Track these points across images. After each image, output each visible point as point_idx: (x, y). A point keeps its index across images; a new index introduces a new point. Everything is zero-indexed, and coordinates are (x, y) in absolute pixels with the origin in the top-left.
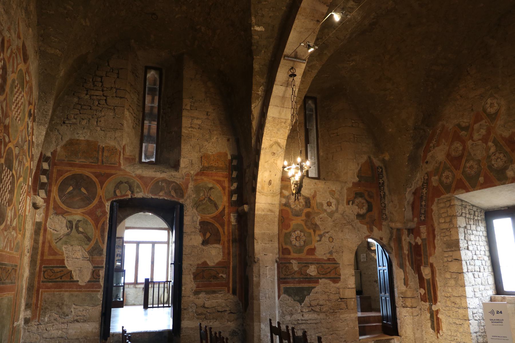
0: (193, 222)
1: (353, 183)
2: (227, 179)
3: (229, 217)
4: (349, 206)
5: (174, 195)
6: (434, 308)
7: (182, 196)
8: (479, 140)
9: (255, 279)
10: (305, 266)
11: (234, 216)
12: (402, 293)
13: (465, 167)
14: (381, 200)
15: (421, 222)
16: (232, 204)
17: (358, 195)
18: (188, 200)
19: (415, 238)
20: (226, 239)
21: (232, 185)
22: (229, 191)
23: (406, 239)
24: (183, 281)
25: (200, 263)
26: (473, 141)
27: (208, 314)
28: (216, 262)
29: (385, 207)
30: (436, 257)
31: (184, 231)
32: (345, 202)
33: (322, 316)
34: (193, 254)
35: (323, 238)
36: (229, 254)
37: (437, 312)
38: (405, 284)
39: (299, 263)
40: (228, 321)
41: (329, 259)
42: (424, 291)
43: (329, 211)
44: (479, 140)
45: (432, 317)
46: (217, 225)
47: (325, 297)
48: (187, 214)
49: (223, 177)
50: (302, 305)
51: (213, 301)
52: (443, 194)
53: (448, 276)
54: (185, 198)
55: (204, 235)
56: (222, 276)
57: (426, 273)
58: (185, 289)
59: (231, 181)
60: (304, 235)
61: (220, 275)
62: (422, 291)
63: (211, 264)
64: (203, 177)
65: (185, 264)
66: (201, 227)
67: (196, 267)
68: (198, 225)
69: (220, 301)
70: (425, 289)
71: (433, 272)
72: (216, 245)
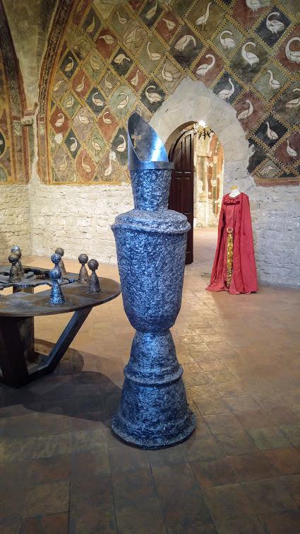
15: (214, 154)
23: (207, 164)
45: (214, 206)
62: (210, 193)
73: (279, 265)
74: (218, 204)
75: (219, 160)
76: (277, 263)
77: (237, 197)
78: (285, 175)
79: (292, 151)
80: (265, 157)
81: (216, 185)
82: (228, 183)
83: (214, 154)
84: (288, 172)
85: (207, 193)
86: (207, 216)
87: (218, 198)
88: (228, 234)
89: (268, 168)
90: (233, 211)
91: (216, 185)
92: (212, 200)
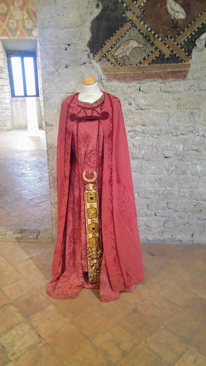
8: (18, 7)
13: (8, 22)
26: (14, 6)
44: (18, 7)
73: (148, 212)
76: (146, 210)
77: (101, 103)
78: (161, 59)
79: (177, 7)
80: (124, 20)
82: (52, 73)
84: (167, 53)
88: (86, 183)
89: (129, 45)
90: (95, 137)
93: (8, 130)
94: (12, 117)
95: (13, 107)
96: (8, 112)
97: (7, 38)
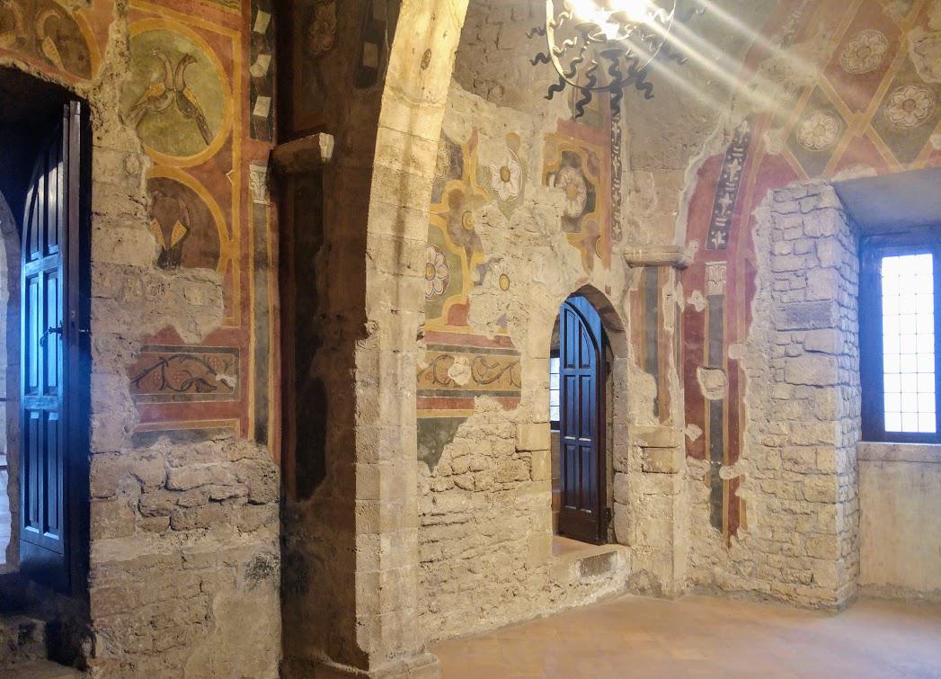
0: (127, 175)
1: (560, 122)
2: (239, 35)
3: (245, 177)
4: (547, 189)
5: (56, 59)
6: (726, 473)
7: (87, 71)
9: (360, 391)
10: (445, 357)
11: (259, 173)
12: (644, 436)
14: (613, 182)
15: (709, 252)
16: (254, 129)
17: (570, 159)
18: (107, 88)
19: (687, 293)
20: (236, 254)
21: (254, 60)
22: (243, 78)
23: (672, 296)
24: (96, 396)
25: (153, 332)
27: (181, 511)
28: (206, 329)
29: (619, 203)
30: (749, 345)
31: (94, 209)
32: (540, 174)
33: (478, 500)
34: (128, 296)
35: (488, 276)
36: (245, 304)
37: (735, 483)
38: (656, 413)
39: (429, 347)
40: (241, 529)
41: (498, 340)
42: (699, 432)
43: (503, 196)
46: (207, 199)
47: (485, 447)
48: (104, 143)
49: (225, 24)
50: (435, 472)
51: (196, 465)
52: (796, 177)
53: (782, 391)
54: (97, 78)
55: (167, 230)
56: (223, 382)
57: (712, 384)
58: (103, 425)
59: (252, 43)
60: (445, 263)
61: (218, 378)
62: (694, 432)
63: (189, 338)
64: (161, 11)
65: (101, 332)
66: (155, 199)
67: (139, 346)
68: (144, 193)
69: (217, 464)
70: (702, 426)
71: (734, 385)
72: (203, 272)
74: (735, 483)
75: (732, 281)
81: (721, 395)
83: (709, 252)
85: (680, 431)
86: (682, 539)
87: (734, 454)
91: (721, 395)
92: (706, 464)
93: (824, 608)
94: (855, 540)
95: (866, 487)
96: (839, 518)
97: (871, 172)
